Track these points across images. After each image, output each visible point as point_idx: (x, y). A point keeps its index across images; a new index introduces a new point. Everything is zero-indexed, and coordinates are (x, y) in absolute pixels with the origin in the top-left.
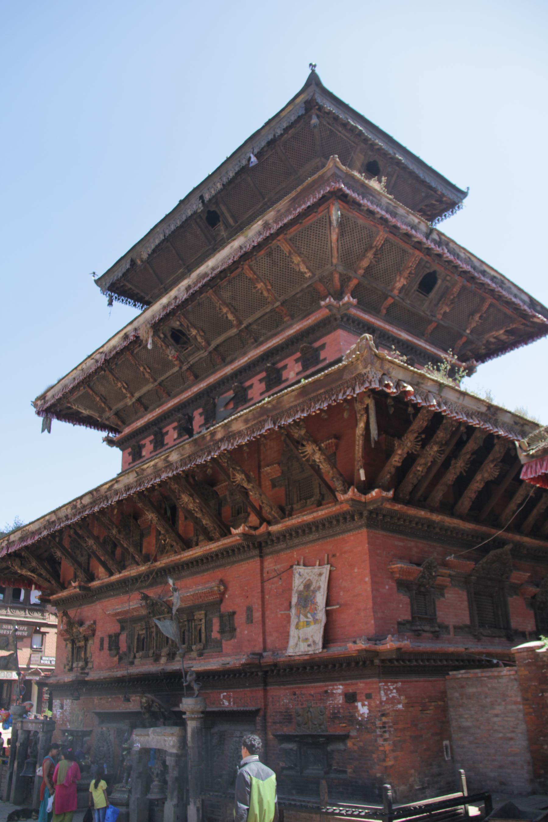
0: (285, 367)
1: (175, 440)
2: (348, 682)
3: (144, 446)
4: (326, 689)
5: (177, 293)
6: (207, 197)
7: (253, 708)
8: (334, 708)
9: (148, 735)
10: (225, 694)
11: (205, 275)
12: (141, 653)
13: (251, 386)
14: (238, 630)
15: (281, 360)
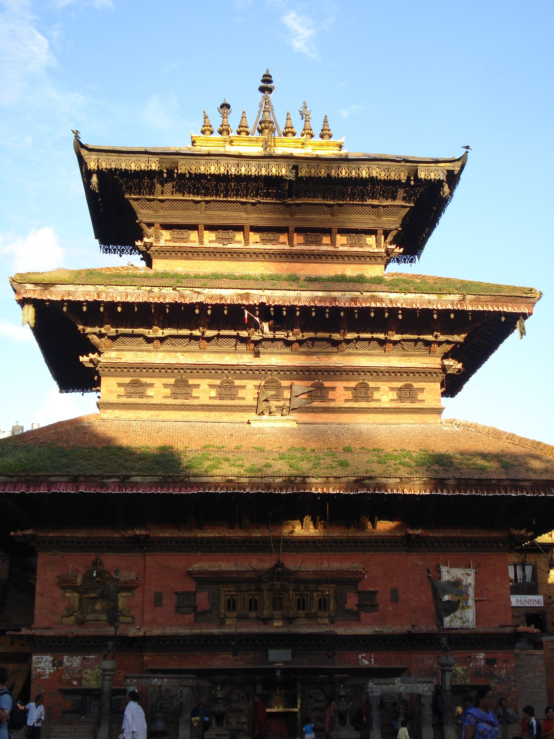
0: (378, 389)
1: (211, 398)
2: (490, 651)
3: (152, 385)
4: (469, 655)
5: (340, 296)
6: (303, 173)
7: (403, 667)
8: (476, 668)
9: (394, 684)
10: (364, 655)
11: (381, 300)
12: (235, 614)
13: (333, 389)
14: (381, 606)
15: (372, 381)
